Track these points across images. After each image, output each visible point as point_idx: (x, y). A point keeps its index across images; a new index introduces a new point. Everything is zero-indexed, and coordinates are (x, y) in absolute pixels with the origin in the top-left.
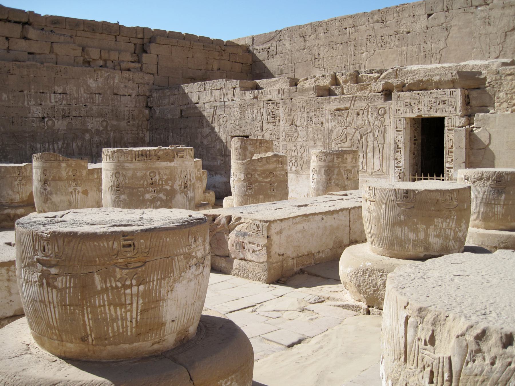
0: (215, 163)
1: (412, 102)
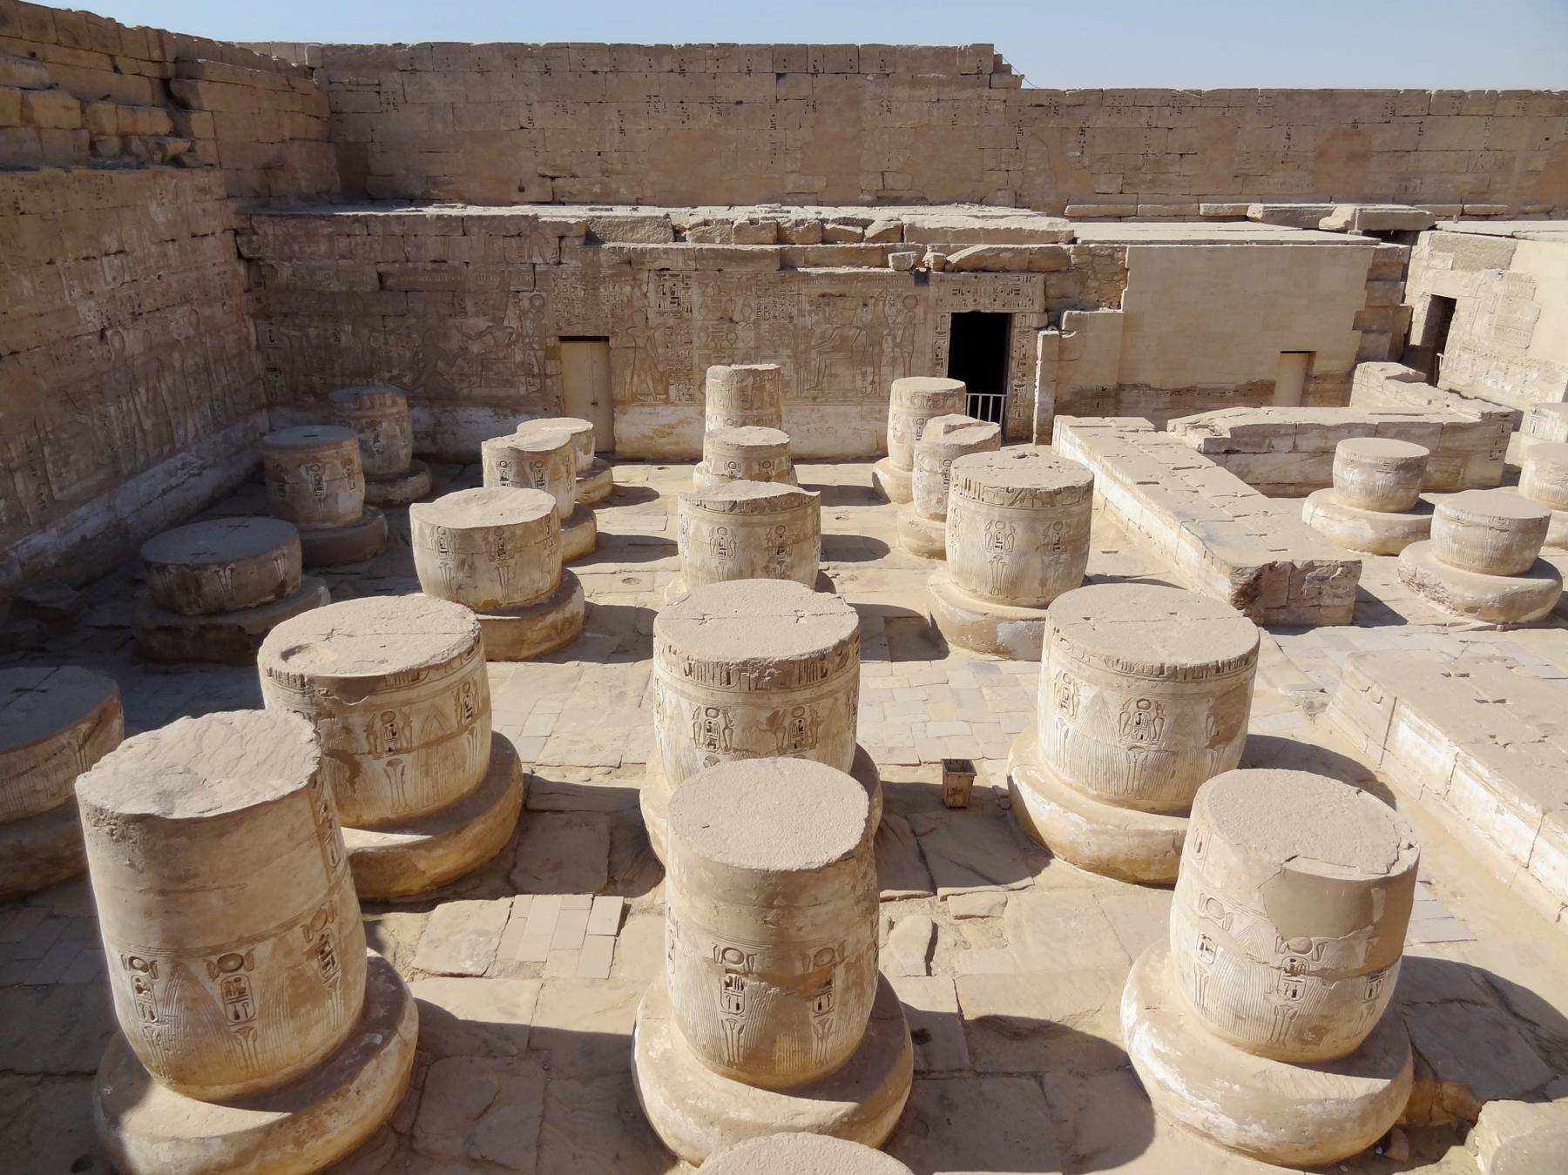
0: (512, 392)
1: (964, 289)
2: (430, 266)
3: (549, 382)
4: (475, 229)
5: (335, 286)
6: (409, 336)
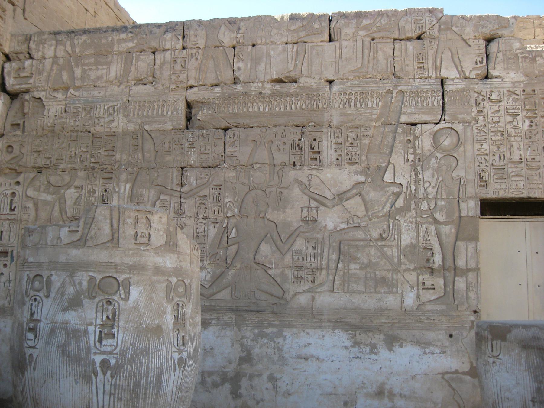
2: (269, 88)
3: (460, 283)
4: (348, 31)
5: (120, 124)
6: (218, 200)
